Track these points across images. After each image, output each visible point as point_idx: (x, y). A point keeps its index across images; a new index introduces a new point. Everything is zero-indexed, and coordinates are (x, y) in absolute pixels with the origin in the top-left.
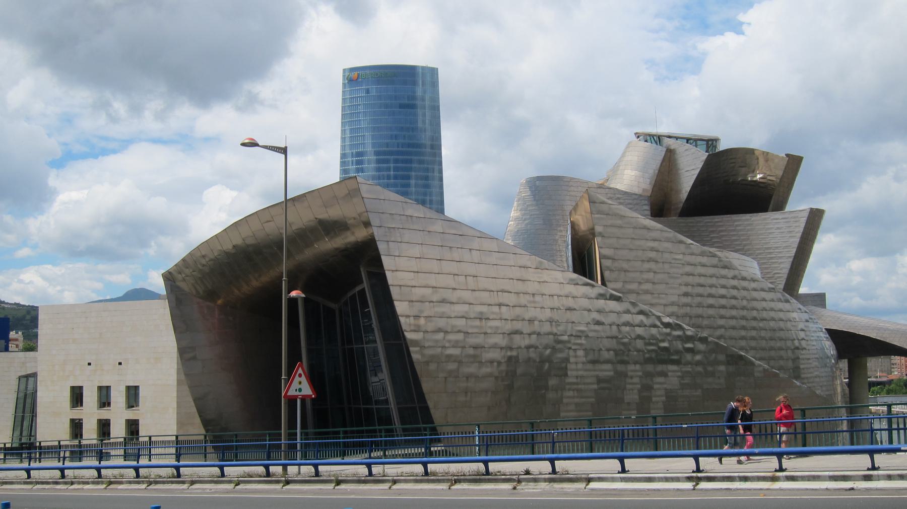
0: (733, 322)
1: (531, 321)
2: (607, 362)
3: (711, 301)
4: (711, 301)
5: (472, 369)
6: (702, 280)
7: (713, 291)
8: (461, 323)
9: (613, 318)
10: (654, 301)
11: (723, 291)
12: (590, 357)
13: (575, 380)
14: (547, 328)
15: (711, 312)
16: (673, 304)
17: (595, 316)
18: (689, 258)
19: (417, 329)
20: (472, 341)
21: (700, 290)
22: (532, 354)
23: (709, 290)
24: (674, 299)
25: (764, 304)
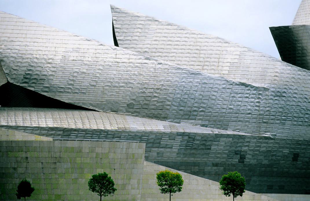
0: (180, 51)
2: (81, 60)
5: (20, 60)
6: (166, 35)
7: (172, 39)
9: (87, 47)
10: (138, 43)
13: (63, 65)
14: (53, 49)
16: (148, 44)
17: (78, 46)
20: (20, 52)
21: (165, 39)
22: (45, 57)
24: (149, 42)
25: (206, 44)
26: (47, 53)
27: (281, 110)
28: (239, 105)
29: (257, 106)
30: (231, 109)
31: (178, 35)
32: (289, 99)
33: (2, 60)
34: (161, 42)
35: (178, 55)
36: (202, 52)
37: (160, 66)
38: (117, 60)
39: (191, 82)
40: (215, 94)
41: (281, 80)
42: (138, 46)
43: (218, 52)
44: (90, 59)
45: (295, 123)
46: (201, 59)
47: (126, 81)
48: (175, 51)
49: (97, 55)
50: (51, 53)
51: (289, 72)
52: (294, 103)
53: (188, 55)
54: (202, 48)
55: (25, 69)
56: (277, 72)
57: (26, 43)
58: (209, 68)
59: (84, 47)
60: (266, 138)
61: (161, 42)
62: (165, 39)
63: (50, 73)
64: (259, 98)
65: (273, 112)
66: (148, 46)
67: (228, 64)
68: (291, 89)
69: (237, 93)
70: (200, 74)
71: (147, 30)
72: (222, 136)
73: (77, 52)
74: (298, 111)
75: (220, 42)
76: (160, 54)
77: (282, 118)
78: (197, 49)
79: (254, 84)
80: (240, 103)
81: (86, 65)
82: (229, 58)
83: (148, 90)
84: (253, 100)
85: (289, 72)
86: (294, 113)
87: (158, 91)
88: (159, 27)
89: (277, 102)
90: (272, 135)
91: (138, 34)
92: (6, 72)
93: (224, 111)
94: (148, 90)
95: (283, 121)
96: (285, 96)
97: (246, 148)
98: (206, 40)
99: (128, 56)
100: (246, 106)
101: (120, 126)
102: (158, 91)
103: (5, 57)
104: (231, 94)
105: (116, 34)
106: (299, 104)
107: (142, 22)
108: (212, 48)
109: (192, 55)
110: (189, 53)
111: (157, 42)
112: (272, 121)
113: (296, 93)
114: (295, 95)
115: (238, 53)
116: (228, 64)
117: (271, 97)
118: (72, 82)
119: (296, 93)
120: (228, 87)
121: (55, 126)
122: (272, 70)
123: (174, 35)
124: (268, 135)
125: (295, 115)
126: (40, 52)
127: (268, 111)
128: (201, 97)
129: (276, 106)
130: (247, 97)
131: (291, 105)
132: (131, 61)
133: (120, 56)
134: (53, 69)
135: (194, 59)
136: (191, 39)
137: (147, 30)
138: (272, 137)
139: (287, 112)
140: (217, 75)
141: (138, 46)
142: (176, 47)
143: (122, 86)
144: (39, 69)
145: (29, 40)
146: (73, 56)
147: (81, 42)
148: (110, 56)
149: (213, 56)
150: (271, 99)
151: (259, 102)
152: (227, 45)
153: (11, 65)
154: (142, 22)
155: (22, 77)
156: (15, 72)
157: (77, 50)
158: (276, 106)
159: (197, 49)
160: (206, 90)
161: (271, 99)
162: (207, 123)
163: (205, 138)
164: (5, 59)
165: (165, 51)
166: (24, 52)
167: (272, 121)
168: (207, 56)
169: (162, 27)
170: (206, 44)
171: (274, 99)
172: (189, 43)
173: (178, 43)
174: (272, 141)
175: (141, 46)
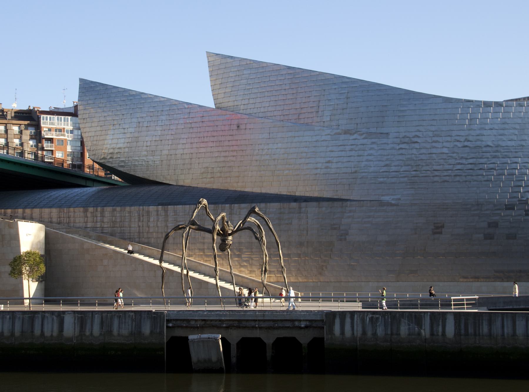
28: (339, 162)
29: (367, 161)
60: (381, 204)
64: (371, 149)
65: (395, 166)
74: (442, 160)
77: (411, 174)
86: (434, 164)
89: (401, 152)
90: (393, 199)
93: (318, 171)
95: (413, 178)
96: (417, 142)
100: (349, 162)
104: (327, 146)
106: (445, 150)
112: (394, 180)
114: (435, 139)
117: (392, 145)
119: (438, 136)
120: (324, 138)
125: (438, 168)
127: (386, 165)
129: (400, 157)
130: (351, 150)
131: (429, 154)
138: (393, 202)
139: (422, 164)
150: (393, 149)
158: (400, 157)
161: (393, 149)
167: (394, 180)
171: (398, 148)
174: (395, 208)
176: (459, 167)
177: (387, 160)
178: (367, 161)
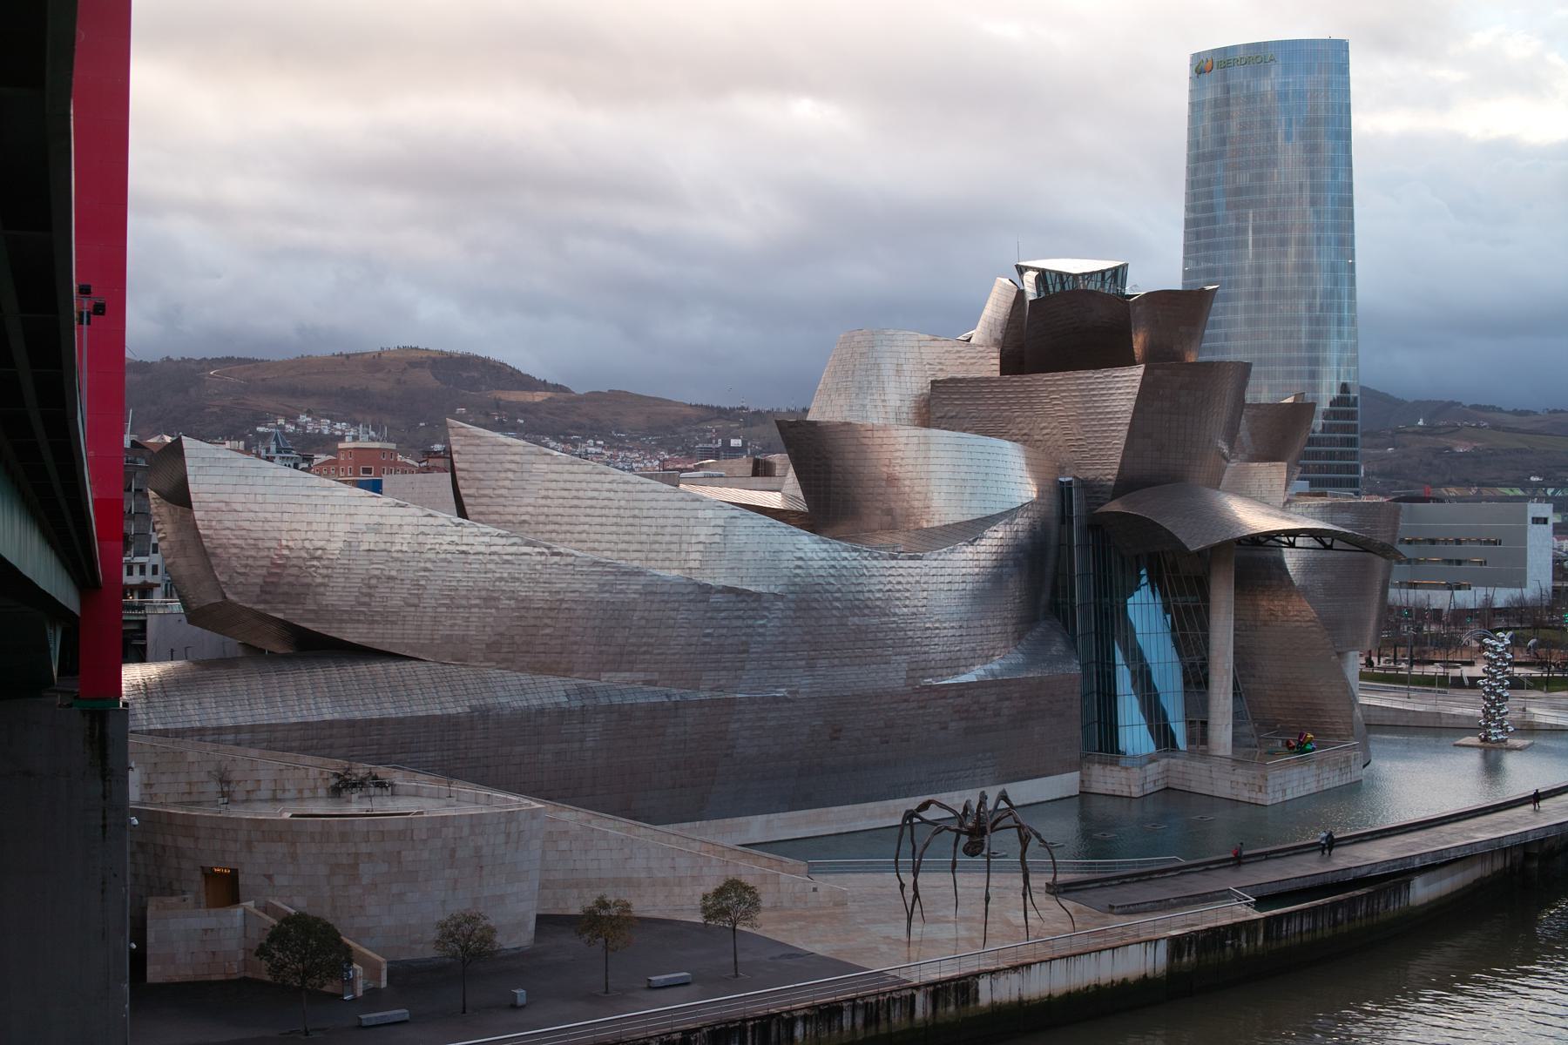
0: (598, 520)
1: (309, 523)
3: (575, 502)
4: (575, 502)
5: (253, 553)
6: (568, 485)
7: (581, 494)
8: (246, 525)
9: (396, 521)
11: (595, 494)
12: (365, 546)
14: (325, 527)
15: (573, 511)
18: (554, 467)
19: (210, 528)
20: (254, 535)
21: (565, 494)
22: (307, 544)
23: (574, 493)
24: (531, 501)
25: (654, 504)
26: (310, 535)
27: (807, 638)
30: (705, 644)
31: (593, 486)
32: (825, 613)
33: (214, 555)
34: (557, 502)
35: (594, 529)
36: (644, 521)
37: (557, 559)
38: (464, 548)
39: (621, 592)
40: (673, 614)
41: (810, 575)
42: (508, 510)
43: (678, 522)
44: (405, 548)
45: (836, 662)
46: (644, 538)
47: (484, 593)
48: (588, 519)
49: (421, 539)
50: (320, 535)
51: (824, 555)
52: (834, 621)
53: (614, 529)
54: (645, 513)
55: (264, 571)
56: (801, 559)
57: (261, 515)
58: (661, 556)
59: (393, 520)
61: (557, 502)
62: (565, 494)
63: (319, 580)
66: (530, 509)
67: (701, 547)
68: (827, 591)
69: (719, 610)
70: (639, 573)
71: (526, 476)
72: (687, 704)
73: (377, 532)
75: (683, 500)
76: (556, 527)
78: (634, 517)
79: (752, 589)
80: (725, 631)
81: (396, 560)
82: (703, 533)
83: (532, 613)
84: (750, 622)
85: (824, 555)
87: (552, 614)
88: (554, 467)
91: (507, 483)
92: (222, 578)
94: (532, 613)
97: (737, 725)
98: (654, 495)
99: (487, 539)
101: (474, 702)
102: (552, 614)
103: (220, 546)
105: (461, 483)
107: (517, 458)
108: (667, 512)
109: (624, 529)
110: (616, 524)
111: (549, 502)
113: (837, 599)
115: (721, 522)
116: (701, 547)
118: (367, 599)
119: (837, 599)
121: (337, 716)
122: (789, 556)
123: (584, 485)
124: (782, 692)
126: (296, 535)
128: (643, 622)
129: (798, 630)
130: (738, 617)
132: (493, 549)
133: (471, 540)
134: (324, 571)
135: (627, 538)
136: (621, 495)
137: (526, 476)
140: (675, 573)
141: (508, 510)
142: (588, 511)
143: (476, 606)
144: (294, 571)
145: (272, 508)
146: (368, 541)
147: (385, 510)
148: (449, 539)
149: (669, 529)
151: (763, 626)
152: (697, 504)
153: (234, 563)
154: (517, 458)
155: (257, 589)
156: (242, 579)
157: (376, 528)
159: (634, 517)
160: (655, 606)
162: (656, 676)
163: (653, 709)
164: (219, 551)
165: (566, 519)
166: (261, 535)
167: (791, 664)
168: (654, 530)
169: (559, 468)
170: (654, 504)
172: (616, 503)
173: (593, 502)
175: (513, 509)
176: (860, 644)
177: (783, 633)
178: (760, 635)
